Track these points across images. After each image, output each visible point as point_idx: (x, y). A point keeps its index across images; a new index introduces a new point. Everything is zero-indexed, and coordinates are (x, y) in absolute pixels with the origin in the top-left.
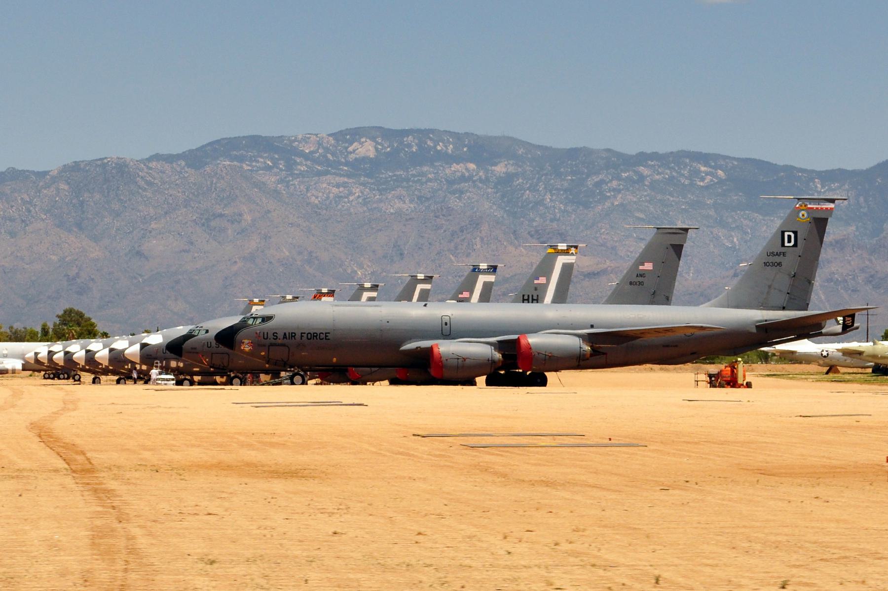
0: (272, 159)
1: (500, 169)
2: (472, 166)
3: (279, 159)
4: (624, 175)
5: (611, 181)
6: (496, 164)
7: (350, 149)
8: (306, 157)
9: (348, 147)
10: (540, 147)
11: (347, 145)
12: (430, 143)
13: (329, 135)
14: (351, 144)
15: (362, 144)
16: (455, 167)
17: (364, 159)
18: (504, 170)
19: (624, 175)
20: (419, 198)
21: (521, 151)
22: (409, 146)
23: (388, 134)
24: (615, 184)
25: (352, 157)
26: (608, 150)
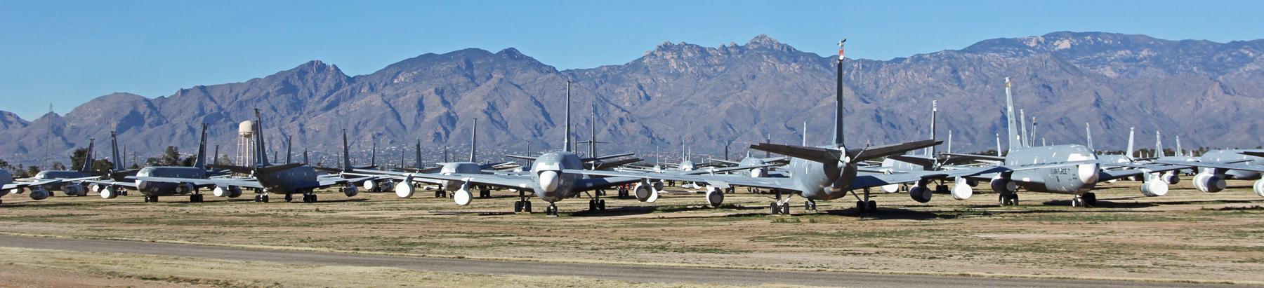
0: (1015, 51)
1: (1144, 53)
2: (1128, 52)
3: (1019, 51)
4: (1234, 54)
5: (1228, 58)
6: (1142, 51)
7: (1055, 44)
8: (1033, 48)
9: (1052, 44)
10: (1160, 40)
11: (1052, 42)
12: (1099, 39)
13: (1043, 36)
14: (1055, 41)
15: (1061, 41)
16: (1119, 53)
17: (1066, 50)
18: (1147, 54)
19: (1234, 54)
20: (1120, 70)
21: (1152, 42)
22: (1089, 41)
23: (1074, 35)
24: (1230, 59)
25: (1056, 49)
26: (1205, 41)
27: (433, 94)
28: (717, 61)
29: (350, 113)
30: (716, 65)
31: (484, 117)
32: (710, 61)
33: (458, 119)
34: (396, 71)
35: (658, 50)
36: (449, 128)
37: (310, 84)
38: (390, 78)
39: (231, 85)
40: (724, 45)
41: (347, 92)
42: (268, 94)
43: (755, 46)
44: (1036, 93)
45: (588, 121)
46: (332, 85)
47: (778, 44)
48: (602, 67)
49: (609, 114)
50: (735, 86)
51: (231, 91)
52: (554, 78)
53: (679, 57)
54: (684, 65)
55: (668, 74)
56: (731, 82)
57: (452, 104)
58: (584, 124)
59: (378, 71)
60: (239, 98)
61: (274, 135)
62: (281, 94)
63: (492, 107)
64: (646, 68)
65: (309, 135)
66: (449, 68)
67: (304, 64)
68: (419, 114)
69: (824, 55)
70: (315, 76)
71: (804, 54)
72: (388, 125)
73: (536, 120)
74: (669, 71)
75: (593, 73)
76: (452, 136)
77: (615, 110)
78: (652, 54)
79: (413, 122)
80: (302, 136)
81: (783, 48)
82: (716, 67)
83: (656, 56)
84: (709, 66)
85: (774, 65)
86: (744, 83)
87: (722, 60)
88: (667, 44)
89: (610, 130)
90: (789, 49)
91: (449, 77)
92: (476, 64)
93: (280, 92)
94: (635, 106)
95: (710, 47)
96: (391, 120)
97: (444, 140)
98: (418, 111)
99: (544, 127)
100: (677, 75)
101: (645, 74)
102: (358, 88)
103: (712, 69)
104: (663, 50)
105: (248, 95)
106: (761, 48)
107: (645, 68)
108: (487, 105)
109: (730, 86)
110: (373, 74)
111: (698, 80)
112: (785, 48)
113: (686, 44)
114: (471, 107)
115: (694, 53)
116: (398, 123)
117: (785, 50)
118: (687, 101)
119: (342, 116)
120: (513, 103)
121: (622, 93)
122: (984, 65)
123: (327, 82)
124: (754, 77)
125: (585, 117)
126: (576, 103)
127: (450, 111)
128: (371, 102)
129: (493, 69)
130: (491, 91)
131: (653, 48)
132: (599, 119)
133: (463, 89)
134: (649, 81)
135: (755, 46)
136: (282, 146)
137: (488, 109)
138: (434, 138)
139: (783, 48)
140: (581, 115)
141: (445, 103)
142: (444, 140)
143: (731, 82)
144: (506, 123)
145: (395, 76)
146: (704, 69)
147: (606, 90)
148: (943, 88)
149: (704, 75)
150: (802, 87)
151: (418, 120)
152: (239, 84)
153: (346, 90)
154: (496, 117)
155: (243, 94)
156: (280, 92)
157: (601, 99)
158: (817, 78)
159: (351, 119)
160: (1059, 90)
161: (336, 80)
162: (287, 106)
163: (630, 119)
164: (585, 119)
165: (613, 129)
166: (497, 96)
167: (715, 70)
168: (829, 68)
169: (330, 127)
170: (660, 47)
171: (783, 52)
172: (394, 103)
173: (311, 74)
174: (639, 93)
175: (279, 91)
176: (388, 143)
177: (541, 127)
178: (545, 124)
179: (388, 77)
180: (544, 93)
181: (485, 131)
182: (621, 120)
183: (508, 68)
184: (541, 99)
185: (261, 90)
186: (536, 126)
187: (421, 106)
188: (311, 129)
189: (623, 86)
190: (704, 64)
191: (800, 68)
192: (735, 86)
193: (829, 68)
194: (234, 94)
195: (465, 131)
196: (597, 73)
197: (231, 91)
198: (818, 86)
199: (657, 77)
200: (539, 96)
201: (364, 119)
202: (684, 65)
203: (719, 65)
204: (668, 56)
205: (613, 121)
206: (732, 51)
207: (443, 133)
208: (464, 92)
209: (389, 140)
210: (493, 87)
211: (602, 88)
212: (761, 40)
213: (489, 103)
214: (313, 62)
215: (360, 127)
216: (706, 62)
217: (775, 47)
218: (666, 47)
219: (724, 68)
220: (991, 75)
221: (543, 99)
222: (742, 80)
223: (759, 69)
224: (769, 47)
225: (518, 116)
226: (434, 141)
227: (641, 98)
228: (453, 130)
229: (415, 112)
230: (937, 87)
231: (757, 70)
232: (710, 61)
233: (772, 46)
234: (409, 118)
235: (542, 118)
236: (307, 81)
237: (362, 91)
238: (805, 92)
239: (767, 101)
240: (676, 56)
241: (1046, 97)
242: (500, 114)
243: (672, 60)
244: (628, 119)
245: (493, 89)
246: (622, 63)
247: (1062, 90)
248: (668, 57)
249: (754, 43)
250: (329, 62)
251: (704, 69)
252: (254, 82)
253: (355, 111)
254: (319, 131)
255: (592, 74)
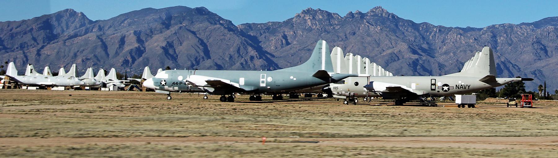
27: (132, 35)
28: (336, 22)
29: (73, 44)
30: (335, 24)
31: (161, 51)
32: (333, 22)
33: (145, 51)
34: (124, 18)
35: (302, 13)
36: (136, 58)
37: (64, 24)
38: (119, 23)
39: (9, 23)
40: (351, 12)
41: (82, 31)
42: (32, 29)
43: (372, 14)
44: (533, 54)
45: (231, 57)
46: (78, 26)
47: (388, 12)
48: (270, 22)
49: (247, 53)
50: (340, 39)
51: (8, 26)
52: (219, 28)
53: (314, 18)
54: (316, 24)
55: (305, 29)
56: (338, 37)
57: (145, 42)
58: (227, 59)
59: (112, 18)
60: (13, 31)
61: (18, 56)
62: (41, 30)
63: (170, 45)
64: (292, 24)
65: (43, 57)
66: (153, 18)
67: (62, 11)
68: (120, 47)
69: (417, 21)
70: (68, 19)
71: (403, 20)
72: (97, 53)
73: (197, 55)
74: (306, 27)
75: (263, 26)
76: (136, 63)
77: (252, 51)
78: (299, 16)
79: (114, 52)
80: (38, 58)
81: (389, 16)
82: (335, 26)
83: (300, 17)
84: (331, 25)
85: (368, 26)
86: (346, 38)
87: (340, 22)
88: (309, 9)
89: (242, 64)
90: (393, 16)
91: (151, 24)
92: (175, 16)
93: (40, 29)
94: (277, 49)
95: (334, 13)
96: (100, 51)
97: (130, 65)
98: (120, 45)
99: (201, 60)
100: (310, 30)
101: (290, 29)
102: (91, 28)
103: (332, 27)
104: (306, 13)
105: (18, 29)
106: (376, 15)
107: (291, 24)
108: (166, 43)
109: (336, 39)
110: (108, 20)
111: (321, 34)
112: (391, 15)
113: (320, 10)
114: (156, 44)
115: (323, 16)
116: (103, 53)
117: (390, 17)
118: (308, 47)
119: (67, 46)
120: (185, 44)
121: (272, 40)
122: (514, 34)
123: (75, 23)
124: (354, 34)
125: (230, 54)
126: (228, 45)
127: (141, 46)
128: (89, 38)
129: (184, 20)
130: (171, 34)
131: (300, 12)
132: (239, 56)
133: (158, 32)
134: (292, 33)
135: (372, 14)
136: (22, 64)
137: (166, 46)
138: (122, 63)
139: (389, 16)
140: (227, 53)
141: (139, 40)
142: (130, 65)
143: (338, 37)
144: (177, 56)
145: (123, 22)
146: (327, 27)
147: (265, 38)
148: (475, 47)
149: (325, 31)
150: (378, 42)
151: (118, 51)
152: (15, 21)
153: (82, 29)
154: (171, 51)
155: (16, 29)
156: (40, 29)
157: (245, 43)
158: (390, 36)
159: (73, 48)
160: (552, 52)
161: (81, 22)
162: (44, 38)
163: (258, 57)
164: (229, 56)
165: (244, 63)
166: (175, 37)
167: (334, 28)
168: (418, 31)
169: (58, 52)
170: (304, 11)
171: (388, 19)
172: (106, 39)
173: (65, 18)
174: (282, 41)
175: (39, 28)
176: (92, 65)
177: (200, 60)
178: (203, 58)
179: (118, 22)
180: (210, 38)
181: (159, 60)
182: (252, 58)
183: (194, 20)
184: (207, 41)
185: (28, 27)
186: (197, 58)
187: (122, 41)
188: (45, 53)
189: (275, 36)
190: (328, 24)
191: (381, 29)
192: (340, 39)
193: (418, 31)
194: (10, 28)
195: (146, 60)
196: (265, 26)
197: (8, 26)
198: (387, 42)
199: (297, 31)
200: (205, 39)
201: (82, 49)
202: (316, 24)
203: (338, 25)
204: (307, 17)
205: (246, 58)
206: (356, 16)
207: (130, 60)
208: (158, 34)
209: (93, 63)
210: (174, 32)
211: (263, 36)
212: (376, 10)
213: (168, 42)
214: (67, 10)
215: (78, 54)
216: (330, 23)
217: (384, 15)
218: (308, 12)
219: (339, 27)
220: (515, 40)
221: (208, 42)
222: (346, 35)
223: (359, 29)
224: (380, 15)
225: (186, 52)
226: (122, 65)
227: (282, 44)
228: (138, 58)
229: (118, 46)
230: (471, 46)
231: (357, 30)
232: (333, 22)
233: (382, 14)
234: (112, 51)
235: (202, 54)
236: (62, 21)
237: (93, 31)
238: (379, 45)
239: (352, 50)
240: (311, 18)
241: (540, 56)
242: (175, 50)
243: (309, 20)
244: (257, 57)
245: (173, 33)
246: (281, 21)
247: (554, 52)
248: (307, 18)
249: (372, 11)
250: (78, 11)
251: (327, 27)
252: (24, 21)
253: (77, 43)
254: (49, 55)
255: (262, 27)
